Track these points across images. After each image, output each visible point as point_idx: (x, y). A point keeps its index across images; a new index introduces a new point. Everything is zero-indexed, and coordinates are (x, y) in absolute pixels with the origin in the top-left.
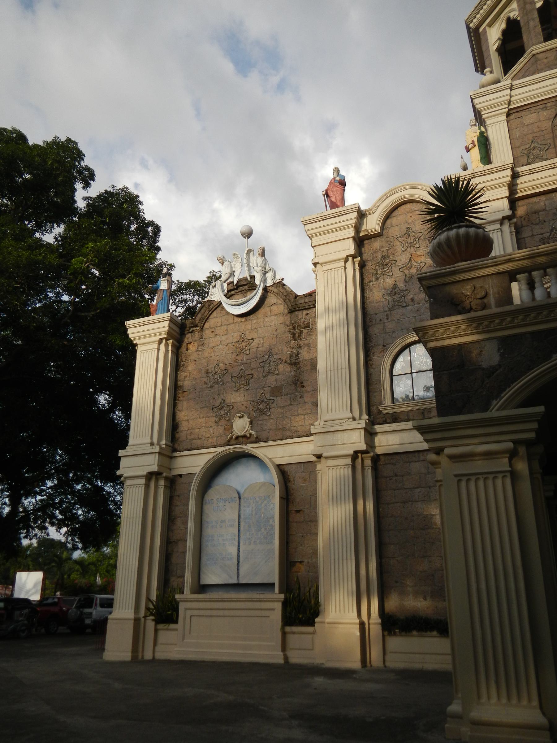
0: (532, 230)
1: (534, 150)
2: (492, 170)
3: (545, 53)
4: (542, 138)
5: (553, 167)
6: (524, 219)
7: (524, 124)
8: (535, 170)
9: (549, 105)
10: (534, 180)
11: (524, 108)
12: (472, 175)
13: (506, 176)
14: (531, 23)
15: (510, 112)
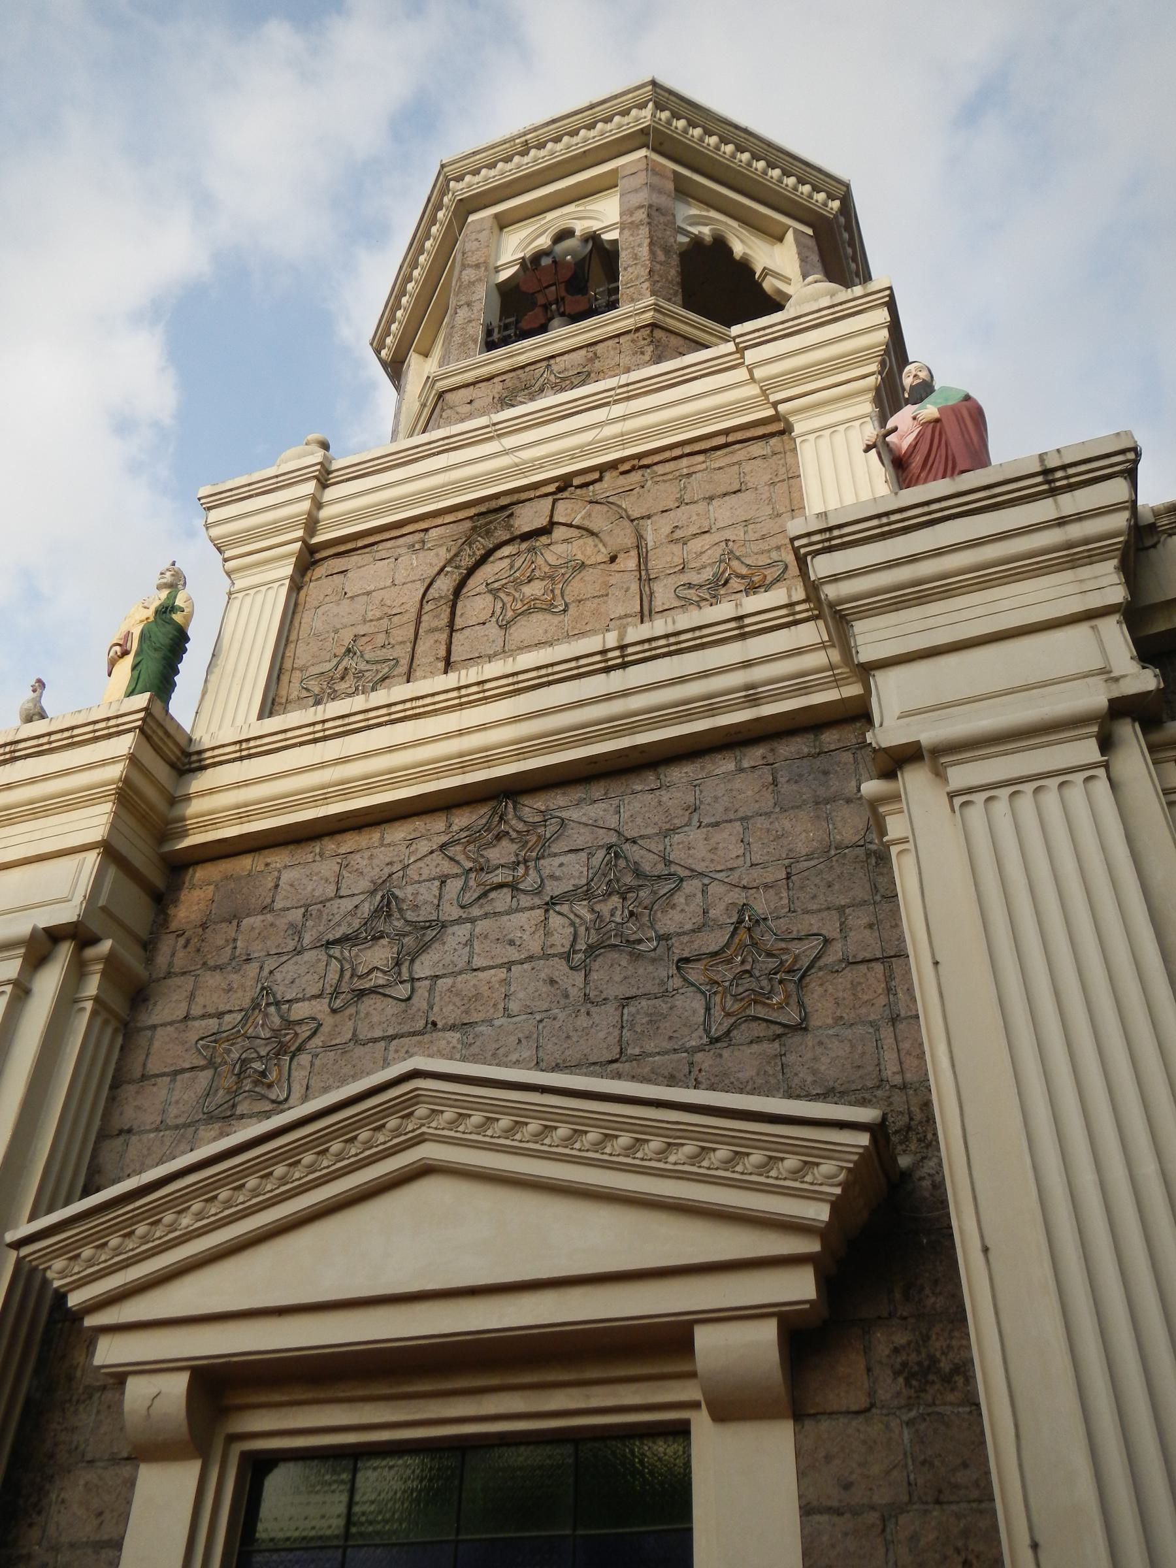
0: (192, 997)
1: (342, 678)
2: (76, 732)
3: (472, 387)
4: (381, 639)
5: (317, 735)
6: (188, 941)
7: (346, 593)
8: (258, 742)
9: (433, 533)
10: (246, 783)
11: (360, 543)
12: (8, 749)
13: (113, 761)
14: (463, 313)
15: (318, 556)
